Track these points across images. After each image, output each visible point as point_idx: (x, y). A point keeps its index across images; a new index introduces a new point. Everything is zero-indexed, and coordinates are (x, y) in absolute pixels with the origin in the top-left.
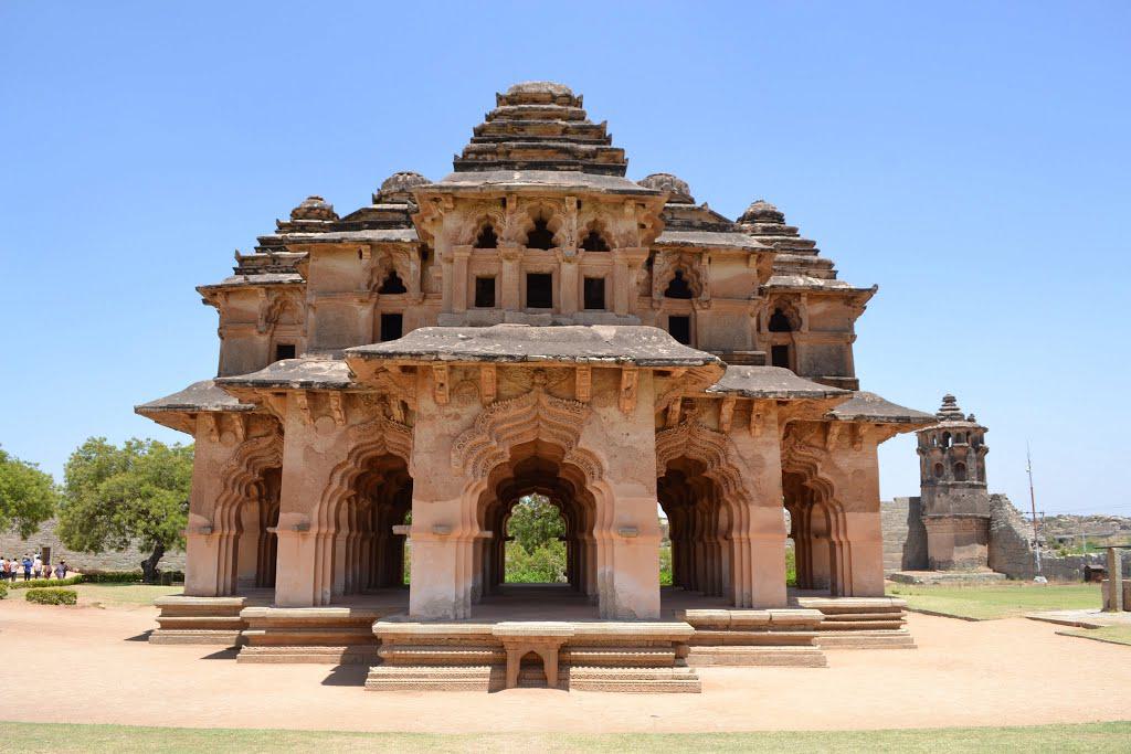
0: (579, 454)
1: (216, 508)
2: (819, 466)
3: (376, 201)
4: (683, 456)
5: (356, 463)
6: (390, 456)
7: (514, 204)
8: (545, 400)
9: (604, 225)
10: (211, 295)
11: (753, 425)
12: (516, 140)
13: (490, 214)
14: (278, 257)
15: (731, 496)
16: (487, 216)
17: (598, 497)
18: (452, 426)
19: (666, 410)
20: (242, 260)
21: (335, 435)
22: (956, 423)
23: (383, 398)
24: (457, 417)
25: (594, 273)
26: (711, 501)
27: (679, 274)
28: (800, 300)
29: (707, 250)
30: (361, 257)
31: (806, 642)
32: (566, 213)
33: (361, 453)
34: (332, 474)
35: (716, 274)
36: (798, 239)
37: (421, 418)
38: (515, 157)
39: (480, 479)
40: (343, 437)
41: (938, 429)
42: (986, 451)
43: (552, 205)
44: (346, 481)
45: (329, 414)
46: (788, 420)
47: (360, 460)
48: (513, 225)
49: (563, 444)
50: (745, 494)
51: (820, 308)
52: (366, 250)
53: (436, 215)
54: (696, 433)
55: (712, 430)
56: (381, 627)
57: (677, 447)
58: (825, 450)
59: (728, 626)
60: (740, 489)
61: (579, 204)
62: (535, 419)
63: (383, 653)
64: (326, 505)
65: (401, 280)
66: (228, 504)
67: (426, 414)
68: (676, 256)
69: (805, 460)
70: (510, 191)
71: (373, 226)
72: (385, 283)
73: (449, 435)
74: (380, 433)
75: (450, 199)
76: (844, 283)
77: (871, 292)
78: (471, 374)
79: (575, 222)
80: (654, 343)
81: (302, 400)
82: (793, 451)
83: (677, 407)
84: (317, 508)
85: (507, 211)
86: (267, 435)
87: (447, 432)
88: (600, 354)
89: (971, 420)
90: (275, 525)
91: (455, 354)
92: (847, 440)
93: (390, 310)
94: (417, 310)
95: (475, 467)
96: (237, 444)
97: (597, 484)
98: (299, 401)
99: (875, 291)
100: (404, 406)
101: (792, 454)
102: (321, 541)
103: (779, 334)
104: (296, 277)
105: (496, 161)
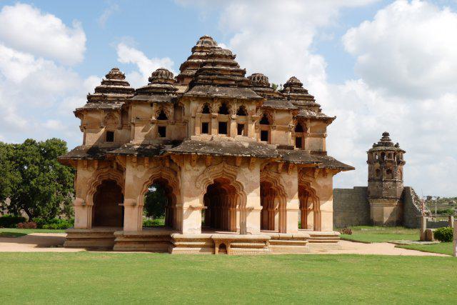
8: (226, 166)
9: (244, 107)
12: (215, 75)
14: (106, 97)
24: (198, 170)
25: (241, 122)
26: (272, 196)
31: (304, 244)
35: (278, 117)
38: (216, 82)
40: (148, 172)
42: (403, 163)
48: (215, 107)
49: (231, 180)
51: (314, 124)
56: (176, 235)
59: (279, 239)
63: (177, 243)
70: (216, 97)
71: (155, 93)
72: (160, 115)
77: (333, 119)
86: (106, 168)
89: (397, 146)
93: (162, 125)
97: (241, 192)
103: (299, 133)
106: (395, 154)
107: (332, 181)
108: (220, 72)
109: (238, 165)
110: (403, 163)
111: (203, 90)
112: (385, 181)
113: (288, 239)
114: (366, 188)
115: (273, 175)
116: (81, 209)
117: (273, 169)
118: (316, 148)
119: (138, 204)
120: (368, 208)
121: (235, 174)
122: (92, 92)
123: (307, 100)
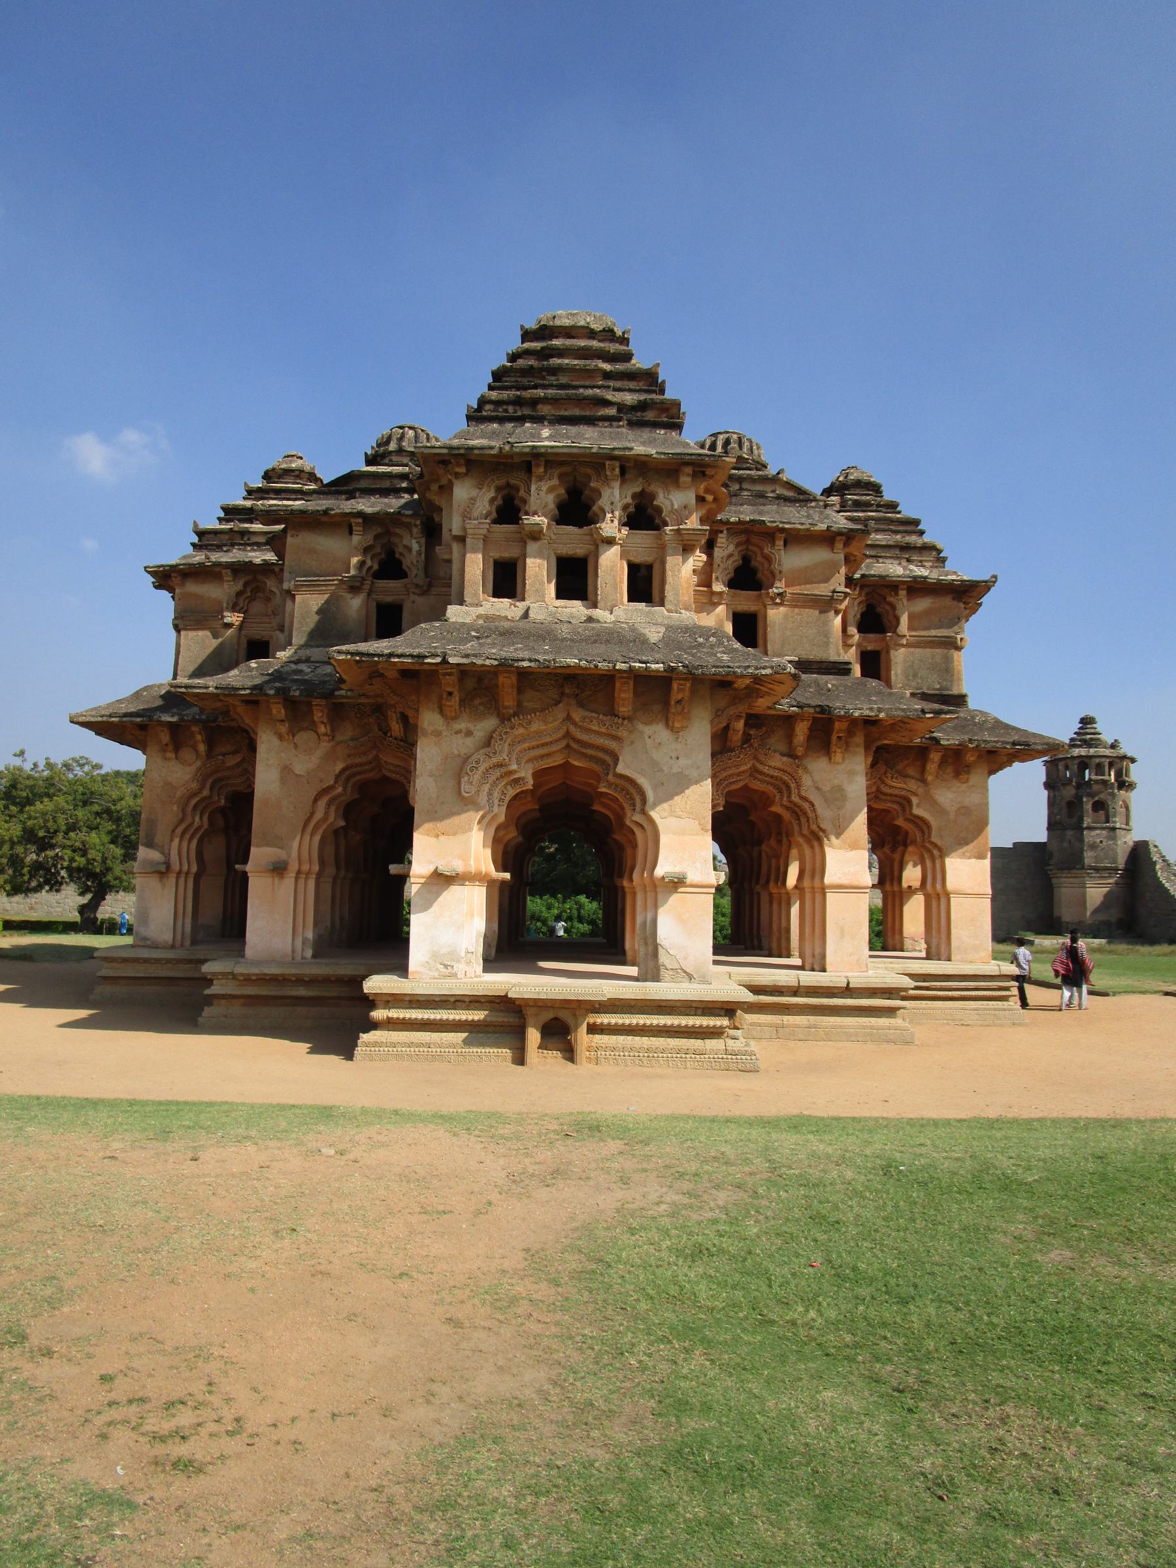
0: (618, 781)
1: (172, 840)
2: (915, 800)
3: (370, 461)
4: (746, 787)
5: (345, 788)
6: (385, 780)
7: (542, 470)
8: (577, 715)
9: (652, 497)
10: (164, 578)
11: (834, 748)
13: (513, 482)
15: (803, 835)
16: (508, 485)
17: (638, 832)
18: (461, 745)
19: (726, 729)
20: (201, 534)
21: (319, 753)
22: (1092, 751)
23: (379, 710)
24: (469, 733)
26: (780, 842)
27: (746, 559)
28: (897, 594)
29: (783, 530)
30: (351, 533)
31: (891, 1012)
32: (607, 481)
33: (355, 775)
34: (315, 800)
36: (898, 516)
37: (425, 735)
38: (544, 409)
39: (496, 809)
41: (1073, 758)
42: (1131, 786)
43: (589, 471)
44: (333, 809)
45: (313, 727)
46: (879, 743)
47: (350, 784)
50: (821, 834)
51: (923, 604)
52: (357, 524)
53: (444, 482)
54: (762, 758)
55: (783, 755)
56: (375, 984)
57: (739, 774)
58: (923, 780)
59: (796, 991)
60: (814, 827)
61: (623, 471)
62: (564, 737)
64: (307, 838)
65: (400, 563)
66: (187, 836)
67: (430, 729)
68: (743, 538)
69: (896, 792)
72: (381, 564)
73: (459, 755)
74: (374, 752)
75: (462, 461)
76: (955, 573)
78: (486, 681)
79: (617, 492)
80: (712, 646)
81: (278, 710)
82: (883, 782)
83: (740, 725)
84: (296, 844)
85: (533, 479)
87: (456, 752)
88: (644, 658)
89: (1113, 746)
90: (245, 861)
91: (467, 656)
92: (950, 770)
93: (389, 599)
94: (420, 600)
95: (490, 794)
96: (199, 763)
97: (637, 817)
98: (274, 711)
99: (995, 582)
100: (404, 719)
101: (882, 786)
102: (301, 882)
103: (872, 636)
104: (271, 557)
105: (519, 414)
106: (1111, 765)
107: (985, 789)
108: (564, 380)
109: (624, 709)
110: (1131, 786)
111: (493, 435)
112: (1089, 828)
113: (830, 992)
114: (1044, 844)
115: (776, 762)
116: (154, 882)
117: (776, 741)
118: (932, 684)
119: (294, 866)
120: (1047, 892)
121: (612, 745)
122: (211, 523)
123: (896, 532)
